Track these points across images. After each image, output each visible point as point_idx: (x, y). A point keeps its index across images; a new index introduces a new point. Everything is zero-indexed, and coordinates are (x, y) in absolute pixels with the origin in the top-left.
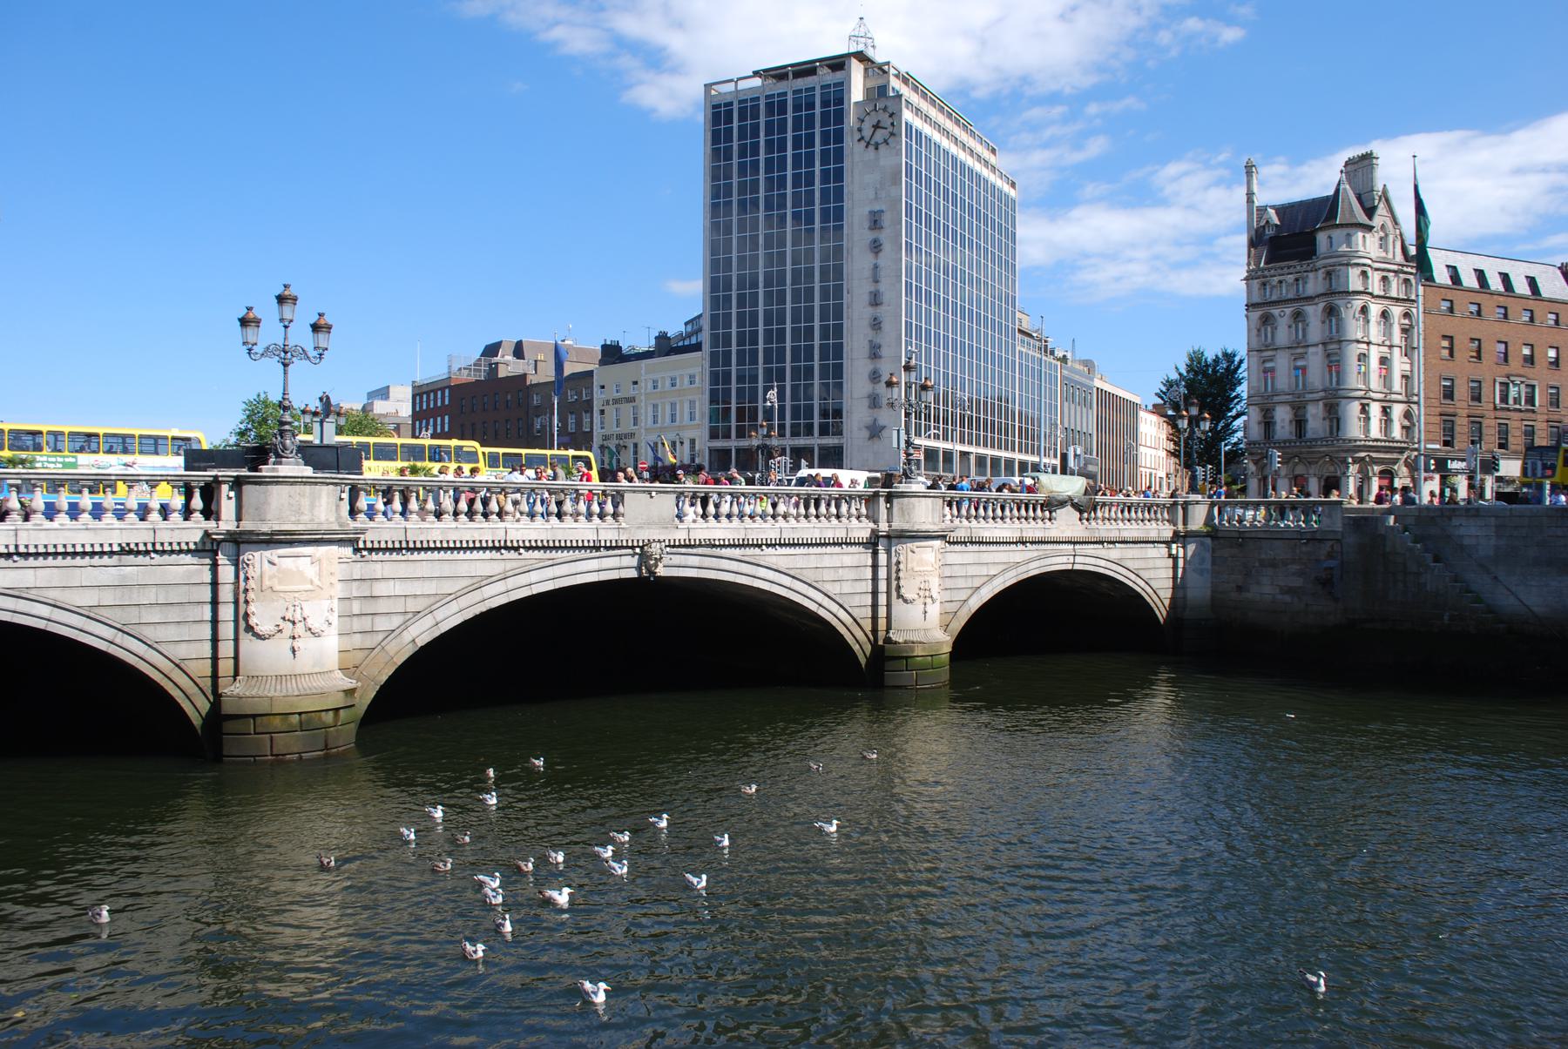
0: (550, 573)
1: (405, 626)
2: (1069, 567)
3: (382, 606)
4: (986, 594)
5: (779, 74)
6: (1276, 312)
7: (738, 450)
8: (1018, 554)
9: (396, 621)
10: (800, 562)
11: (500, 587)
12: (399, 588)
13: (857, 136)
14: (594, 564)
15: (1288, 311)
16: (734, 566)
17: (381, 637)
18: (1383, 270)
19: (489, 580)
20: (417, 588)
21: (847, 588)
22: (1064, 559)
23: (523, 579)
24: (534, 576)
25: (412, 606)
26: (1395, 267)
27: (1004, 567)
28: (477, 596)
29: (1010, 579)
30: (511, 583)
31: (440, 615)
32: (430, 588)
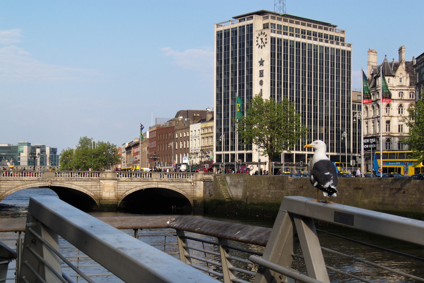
0: (30, 185)
1: (6, 192)
2: (157, 187)
3: (2, 189)
4: (131, 192)
5: (241, 18)
6: (368, 106)
7: (247, 154)
8: (140, 184)
9: (4, 191)
10: (82, 184)
11: (22, 187)
12: (5, 186)
13: (257, 43)
14: (39, 184)
15: (371, 105)
16: (67, 184)
17: (2, 193)
18: (400, 90)
19: (20, 186)
20: (8, 187)
21: (93, 189)
22: (155, 185)
23: (26, 186)
24: (28, 185)
25: (7, 189)
26: (406, 88)
27: (135, 187)
28: (18, 188)
29: (138, 189)
30: (24, 186)
31: (12, 190)
32: (10, 187)
